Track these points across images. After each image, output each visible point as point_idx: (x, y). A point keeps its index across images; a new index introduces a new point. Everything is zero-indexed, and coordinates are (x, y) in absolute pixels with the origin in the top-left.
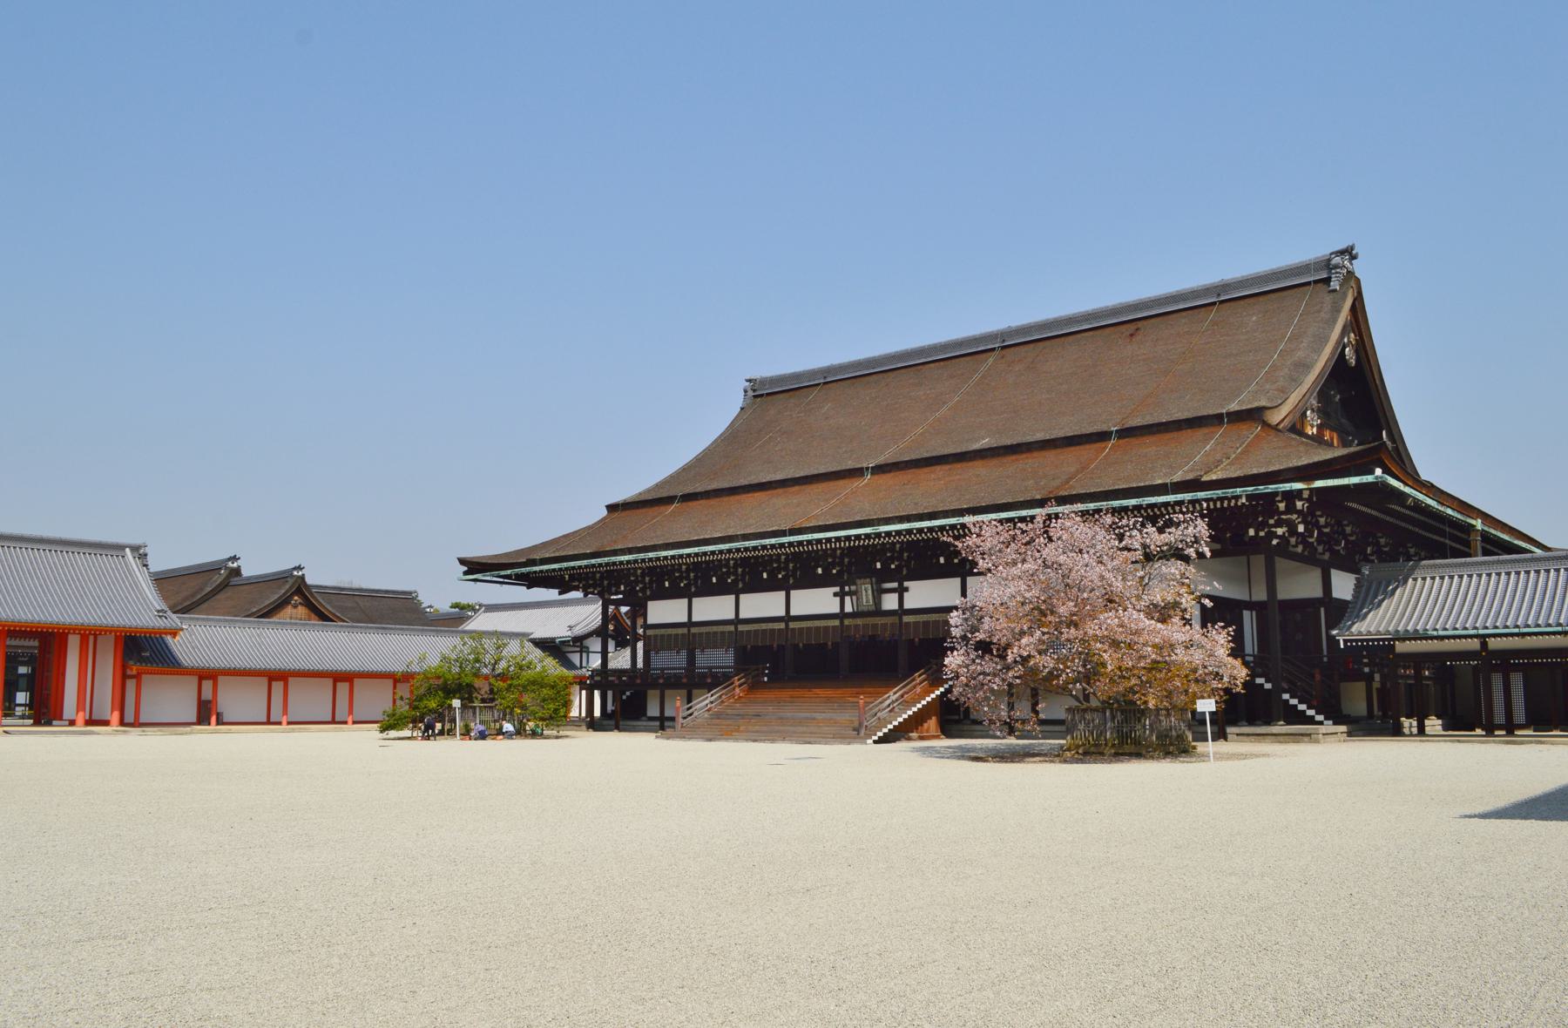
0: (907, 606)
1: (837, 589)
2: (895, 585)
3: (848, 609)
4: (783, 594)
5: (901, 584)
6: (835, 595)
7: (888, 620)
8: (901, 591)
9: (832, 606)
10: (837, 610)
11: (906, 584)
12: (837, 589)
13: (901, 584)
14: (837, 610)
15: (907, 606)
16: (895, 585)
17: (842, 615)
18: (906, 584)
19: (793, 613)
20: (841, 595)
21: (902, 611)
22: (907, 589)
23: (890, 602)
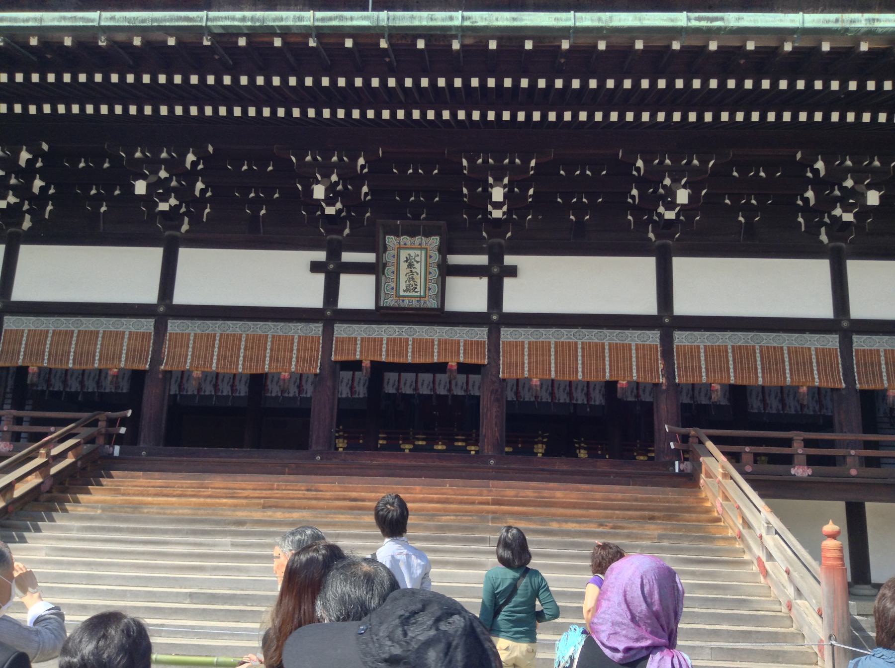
0: (512, 304)
1: (320, 256)
2: (482, 260)
3: (357, 292)
4: (155, 255)
5: (496, 258)
6: (315, 267)
7: (462, 334)
8: (497, 277)
9: (309, 293)
10: (316, 300)
11: (509, 260)
12: (320, 256)
13: (496, 258)
14: (316, 300)
15: (512, 304)
16: (482, 260)
17: (330, 314)
18: (509, 260)
19: (182, 296)
20: (332, 273)
21: (495, 318)
22: (512, 272)
23: (469, 295)
